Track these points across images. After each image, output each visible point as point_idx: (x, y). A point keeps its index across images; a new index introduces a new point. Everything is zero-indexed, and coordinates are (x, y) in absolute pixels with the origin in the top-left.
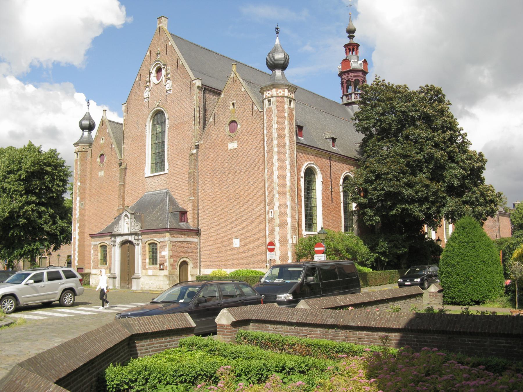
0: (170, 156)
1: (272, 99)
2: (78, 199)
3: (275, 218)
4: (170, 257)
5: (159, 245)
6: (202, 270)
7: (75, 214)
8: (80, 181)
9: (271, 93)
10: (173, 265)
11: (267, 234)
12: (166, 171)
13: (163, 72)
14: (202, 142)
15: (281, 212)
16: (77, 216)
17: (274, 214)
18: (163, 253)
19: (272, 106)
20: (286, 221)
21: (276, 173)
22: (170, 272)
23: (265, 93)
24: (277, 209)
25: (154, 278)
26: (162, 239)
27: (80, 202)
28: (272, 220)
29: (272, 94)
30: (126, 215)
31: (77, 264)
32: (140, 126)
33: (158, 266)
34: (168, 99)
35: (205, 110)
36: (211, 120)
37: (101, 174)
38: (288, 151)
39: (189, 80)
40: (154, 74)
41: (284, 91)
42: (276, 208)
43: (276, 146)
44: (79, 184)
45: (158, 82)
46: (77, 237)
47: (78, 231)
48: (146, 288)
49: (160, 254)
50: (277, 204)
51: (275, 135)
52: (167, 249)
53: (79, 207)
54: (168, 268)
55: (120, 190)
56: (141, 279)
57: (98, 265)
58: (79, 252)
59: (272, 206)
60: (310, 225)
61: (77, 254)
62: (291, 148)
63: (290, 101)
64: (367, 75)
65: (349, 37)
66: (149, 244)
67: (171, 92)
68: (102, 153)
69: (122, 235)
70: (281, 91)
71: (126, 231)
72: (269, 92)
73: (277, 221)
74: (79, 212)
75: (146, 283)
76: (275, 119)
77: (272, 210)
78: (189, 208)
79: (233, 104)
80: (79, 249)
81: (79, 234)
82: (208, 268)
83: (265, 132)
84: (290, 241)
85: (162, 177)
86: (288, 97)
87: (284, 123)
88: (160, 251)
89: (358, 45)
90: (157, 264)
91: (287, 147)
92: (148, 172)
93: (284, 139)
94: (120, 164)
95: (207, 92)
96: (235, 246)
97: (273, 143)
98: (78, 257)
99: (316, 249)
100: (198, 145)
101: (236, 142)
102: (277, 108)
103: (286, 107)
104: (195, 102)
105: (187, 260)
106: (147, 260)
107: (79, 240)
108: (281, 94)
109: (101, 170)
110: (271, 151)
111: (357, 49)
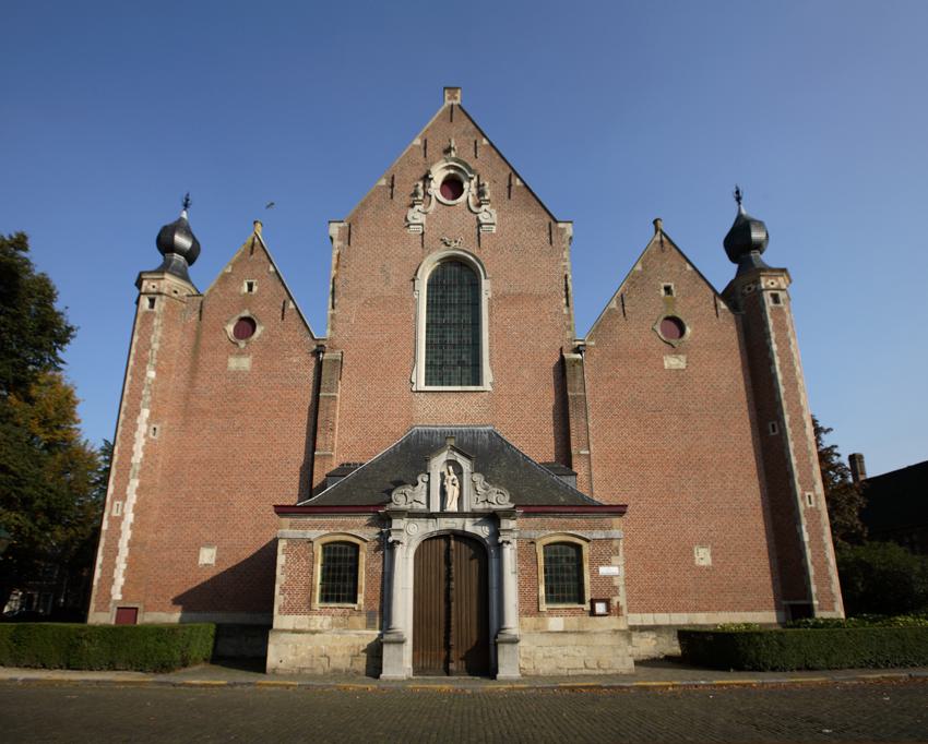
1: (779, 292)
2: (145, 413)
3: (820, 508)
4: (629, 580)
5: (586, 550)
12: (487, 385)
13: (469, 188)
14: (593, 343)
18: (604, 570)
19: (782, 305)
23: (763, 279)
25: (572, 639)
27: (149, 423)
31: (117, 596)
32: (393, 278)
33: (587, 607)
46: (130, 517)
47: (132, 499)
48: (546, 668)
49: (594, 574)
52: (619, 560)
53: (146, 436)
56: (520, 644)
57: (310, 600)
58: (130, 562)
67: (494, 231)
74: (145, 449)
75: (540, 655)
77: (811, 494)
79: (667, 289)
80: (131, 553)
81: (136, 510)
88: (592, 565)
98: (129, 573)
107: (132, 526)
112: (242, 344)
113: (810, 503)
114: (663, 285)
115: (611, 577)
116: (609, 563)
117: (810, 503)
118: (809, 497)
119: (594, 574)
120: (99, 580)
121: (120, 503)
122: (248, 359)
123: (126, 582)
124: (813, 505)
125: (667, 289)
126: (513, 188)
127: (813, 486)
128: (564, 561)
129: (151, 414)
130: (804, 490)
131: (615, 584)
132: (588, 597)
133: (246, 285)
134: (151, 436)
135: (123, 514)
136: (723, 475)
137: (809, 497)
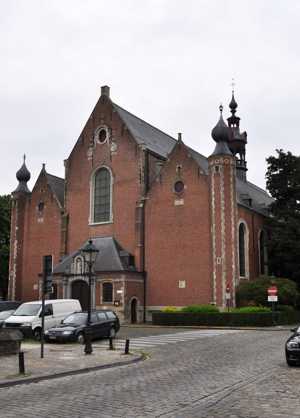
0: (115, 208)
2: (16, 242)
3: (222, 264)
4: (126, 295)
6: (147, 307)
7: (13, 255)
8: (18, 226)
9: (218, 161)
10: (127, 302)
11: (215, 277)
13: (108, 134)
14: (148, 198)
15: (227, 260)
16: (15, 258)
17: (221, 261)
20: (232, 267)
21: (223, 227)
22: (125, 308)
24: (224, 257)
26: (118, 280)
27: (17, 244)
28: (219, 267)
29: (220, 162)
30: (79, 258)
33: (113, 303)
34: (113, 159)
35: (148, 171)
36: (157, 180)
37: (41, 220)
38: (233, 210)
39: (135, 144)
40: (97, 137)
41: (229, 160)
42: (223, 256)
43: (223, 205)
44: (17, 228)
45: (102, 143)
46: (15, 276)
47: (15, 270)
50: (224, 253)
51: (223, 196)
52: (123, 288)
53: (17, 249)
54: (124, 305)
55: (62, 236)
58: (15, 289)
59: (219, 254)
60: (242, 273)
61: (14, 291)
62: (235, 207)
63: (234, 168)
64: (246, 145)
65: (231, 111)
66: (103, 284)
68: (41, 201)
69: (73, 275)
70: (228, 160)
71: (79, 272)
72: (218, 160)
73: (224, 267)
74: (17, 254)
76: (222, 183)
77: (220, 258)
78: (137, 254)
82: (154, 305)
83: (213, 193)
84: (234, 285)
85: (107, 226)
86: (232, 165)
87: (230, 186)
89: (239, 119)
90: (112, 301)
91: (232, 207)
92: (91, 222)
93: (230, 200)
94: (63, 213)
95: (149, 155)
96: (180, 287)
97: (221, 202)
98: (15, 293)
99: (269, 291)
100: (144, 200)
101: (182, 200)
102: (224, 174)
103: (231, 173)
104: (141, 163)
105: (137, 298)
106: (101, 298)
107: (16, 279)
108: (228, 162)
109: (41, 217)
110: (218, 209)
111: (239, 122)
112: (41, 213)
113: (219, 262)
114: (177, 166)
115: (120, 294)
116: (120, 290)
117: (219, 262)
118: (219, 259)
119: (116, 293)
120: (9, 295)
121: (12, 271)
122: (43, 218)
123: (15, 296)
124: (220, 263)
125: (179, 167)
126: (124, 131)
127: (221, 255)
128: (109, 288)
129: (18, 242)
130: (217, 257)
131: (121, 296)
132: (113, 300)
133: (41, 190)
134: (19, 249)
135: (13, 275)
136: (193, 250)
137: (219, 259)
